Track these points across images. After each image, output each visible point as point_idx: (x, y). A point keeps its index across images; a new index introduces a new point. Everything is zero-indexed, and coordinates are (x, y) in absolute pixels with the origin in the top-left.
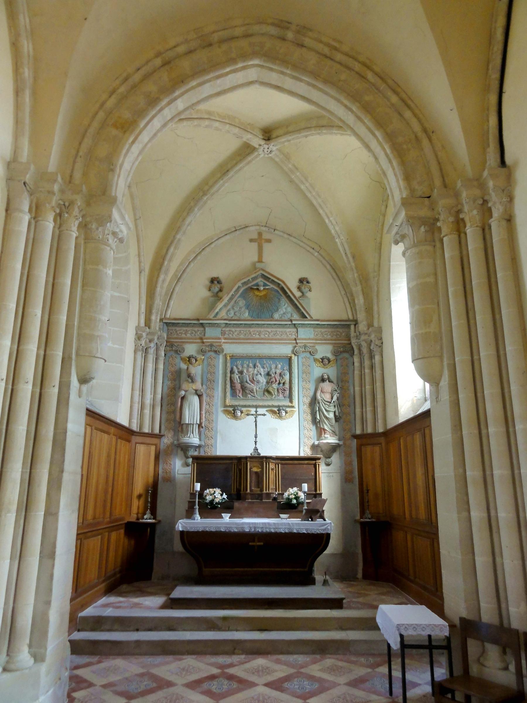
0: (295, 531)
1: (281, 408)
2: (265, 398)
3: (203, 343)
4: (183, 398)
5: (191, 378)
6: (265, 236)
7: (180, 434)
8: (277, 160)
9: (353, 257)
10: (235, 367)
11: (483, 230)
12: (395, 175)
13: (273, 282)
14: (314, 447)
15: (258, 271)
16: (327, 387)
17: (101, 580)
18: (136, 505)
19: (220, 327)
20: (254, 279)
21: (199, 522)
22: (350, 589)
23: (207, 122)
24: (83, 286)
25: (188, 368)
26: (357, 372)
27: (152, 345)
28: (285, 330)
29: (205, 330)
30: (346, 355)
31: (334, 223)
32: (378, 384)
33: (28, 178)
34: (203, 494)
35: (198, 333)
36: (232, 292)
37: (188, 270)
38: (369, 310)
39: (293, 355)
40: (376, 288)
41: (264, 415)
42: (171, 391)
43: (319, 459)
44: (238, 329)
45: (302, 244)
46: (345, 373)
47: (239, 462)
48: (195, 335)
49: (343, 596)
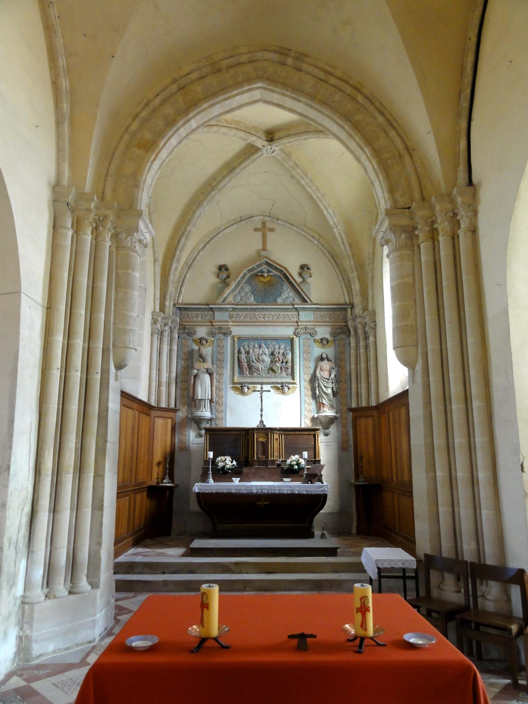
0: (296, 492)
1: (284, 385)
2: (269, 375)
3: (213, 326)
4: (195, 376)
5: (202, 358)
6: (269, 225)
7: (193, 408)
8: (279, 158)
9: (350, 246)
10: (242, 348)
11: (453, 238)
12: (381, 186)
13: (276, 269)
14: (313, 420)
15: (263, 259)
16: (326, 365)
17: (130, 534)
18: (156, 471)
19: (228, 311)
20: (258, 266)
21: (212, 485)
22: (344, 542)
23: (215, 129)
24: (116, 288)
25: (199, 349)
26: (353, 352)
27: (167, 328)
28: (287, 313)
29: (214, 314)
30: (343, 336)
31: (332, 214)
32: (372, 363)
33: (70, 199)
34: (215, 461)
35: (208, 317)
36: (239, 279)
37: (198, 258)
38: (364, 295)
39: (295, 337)
40: (370, 275)
41: (269, 391)
42: (185, 370)
43: (318, 430)
44: (244, 313)
45: (302, 233)
46: (342, 353)
47: (248, 432)
48: (205, 319)
49: (337, 546)
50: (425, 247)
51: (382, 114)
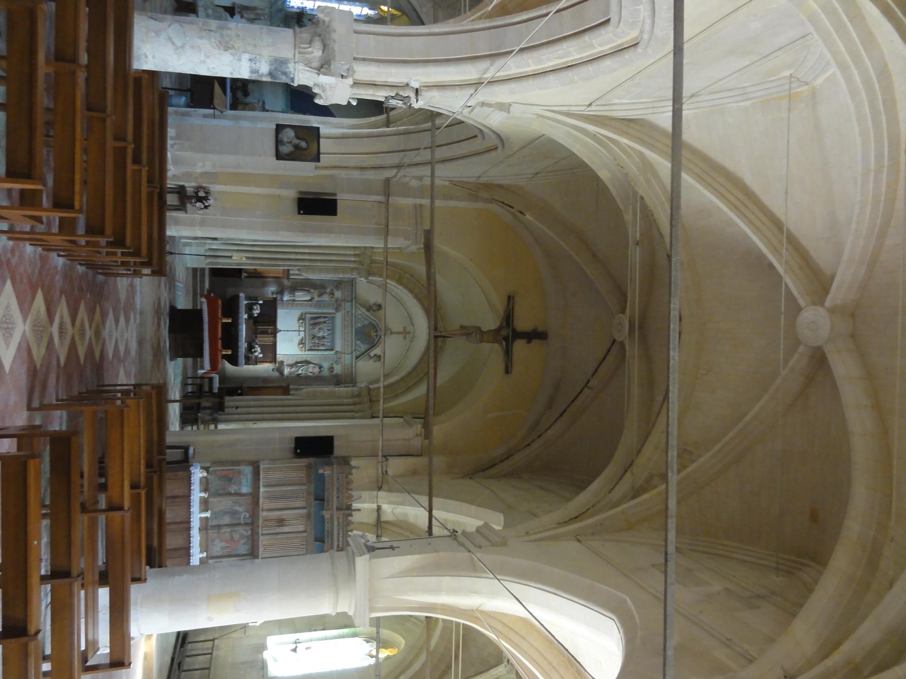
6: (408, 336)
14: (282, 362)
16: (317, 370)
21: (244, 302)
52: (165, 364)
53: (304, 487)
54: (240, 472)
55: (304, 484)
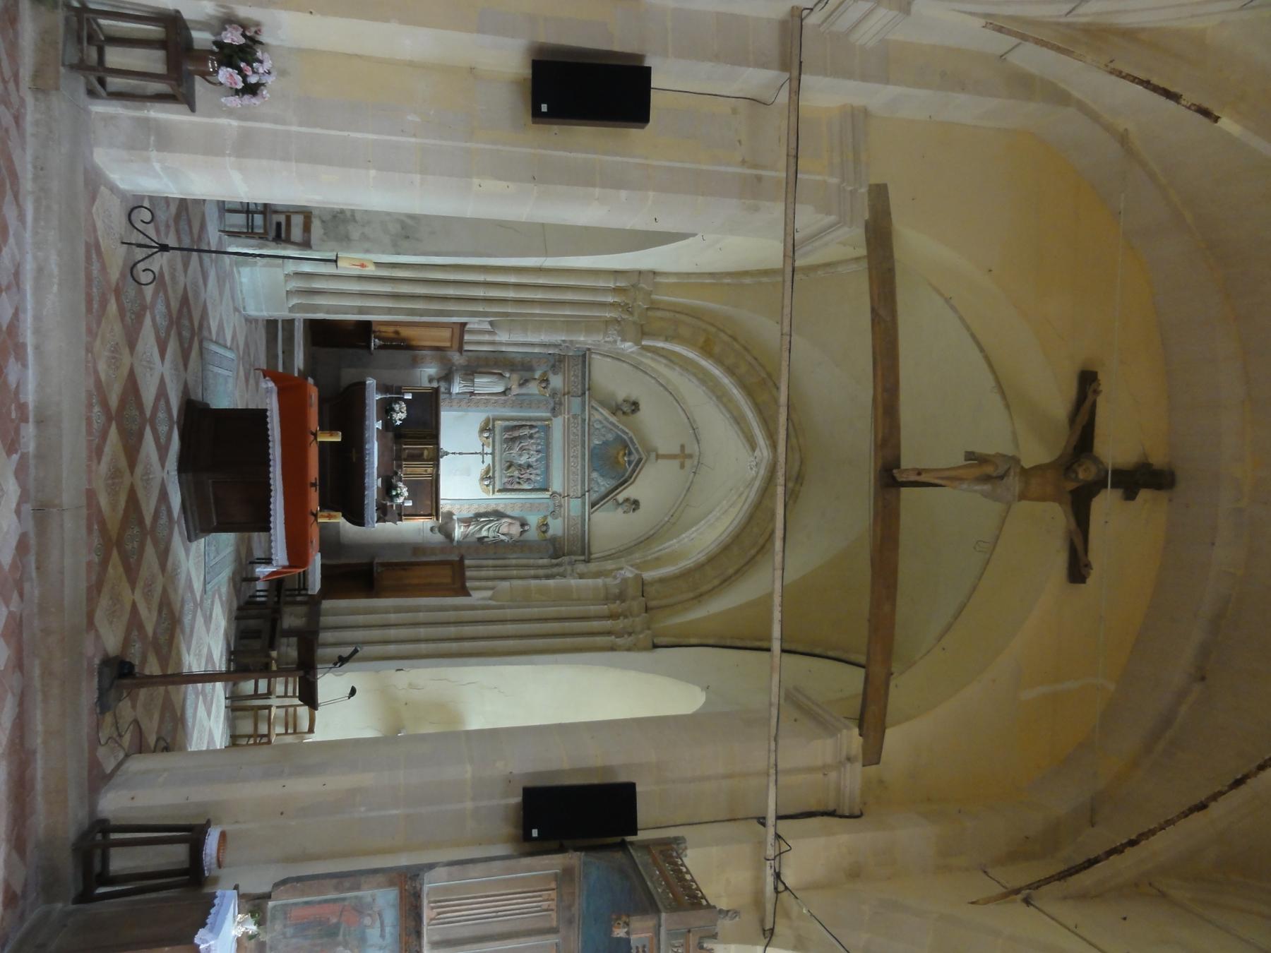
6: (688, 463)
13: (634, 471)
14: (450, 515)
16: (515, 530)
20: (637, 450)
21: (374, 397)
30: (551, 551)
47: (434, 437)
50: (604, 609)
51: (736, 572)
52: (164, 554)
53: (552, 939)
54: (360, 909)
55: (553, 931)
